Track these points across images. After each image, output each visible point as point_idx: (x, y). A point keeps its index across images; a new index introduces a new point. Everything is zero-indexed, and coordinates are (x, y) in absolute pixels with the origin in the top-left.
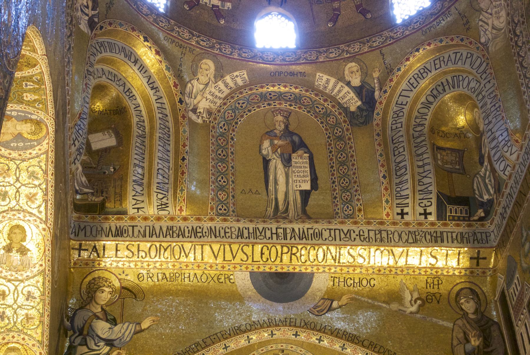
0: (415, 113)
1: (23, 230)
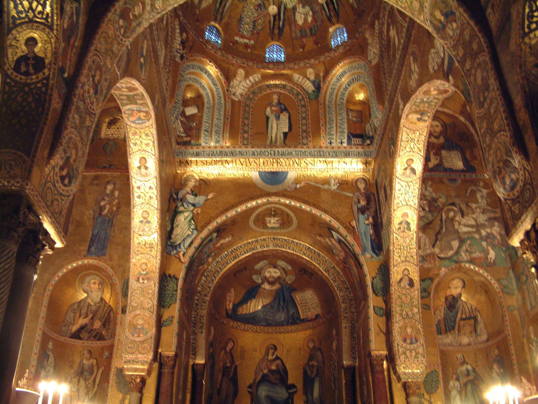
0: (340, 93)
1: (145, 159)
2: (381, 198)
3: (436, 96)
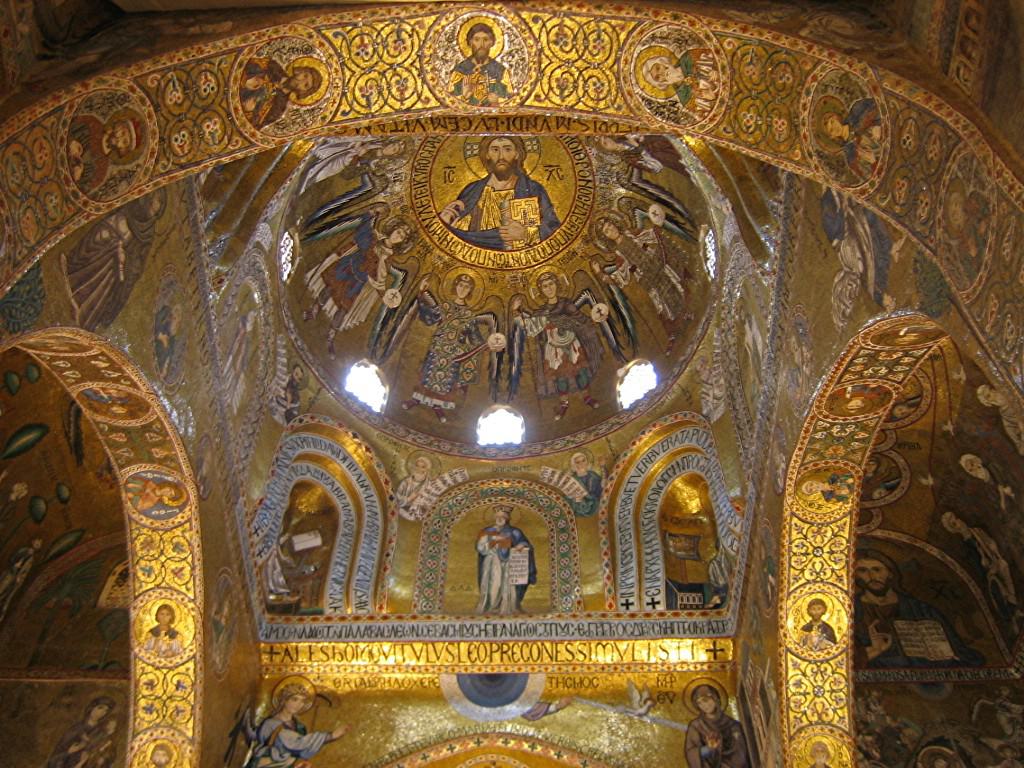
2: (756, 723)
3: (861, 418)
